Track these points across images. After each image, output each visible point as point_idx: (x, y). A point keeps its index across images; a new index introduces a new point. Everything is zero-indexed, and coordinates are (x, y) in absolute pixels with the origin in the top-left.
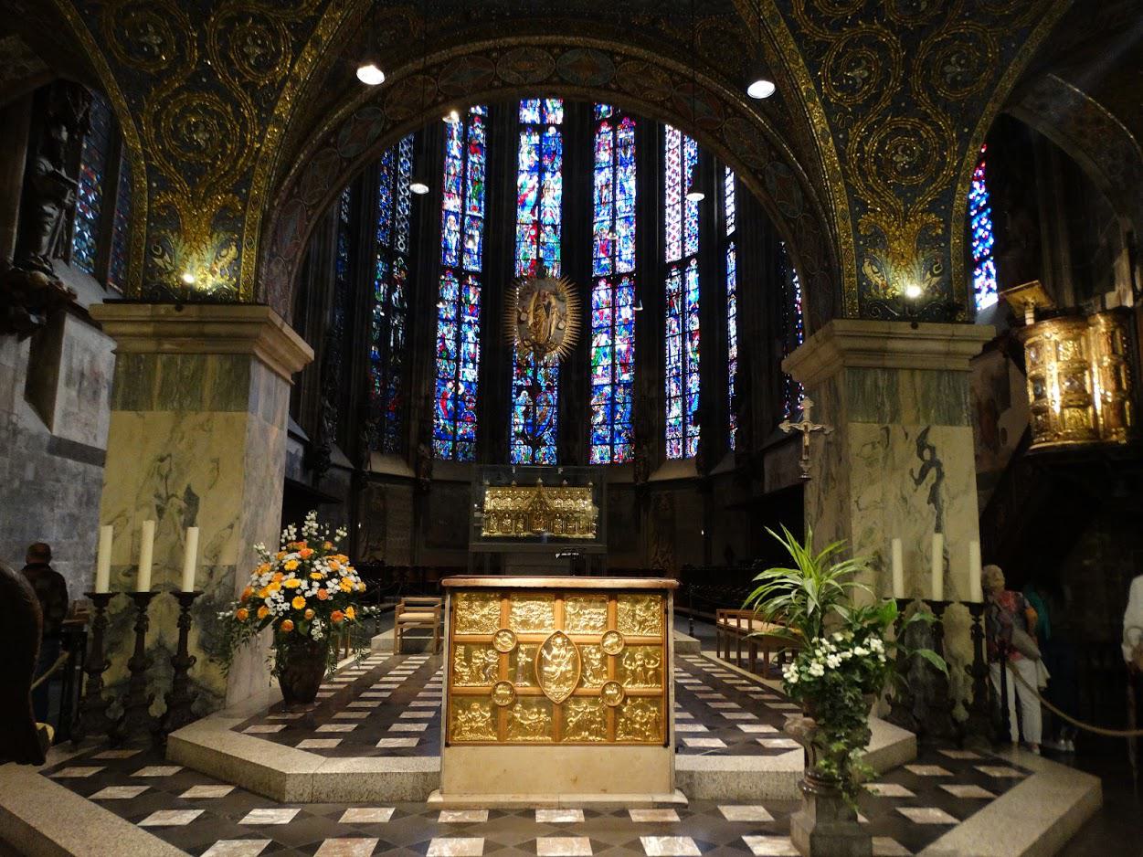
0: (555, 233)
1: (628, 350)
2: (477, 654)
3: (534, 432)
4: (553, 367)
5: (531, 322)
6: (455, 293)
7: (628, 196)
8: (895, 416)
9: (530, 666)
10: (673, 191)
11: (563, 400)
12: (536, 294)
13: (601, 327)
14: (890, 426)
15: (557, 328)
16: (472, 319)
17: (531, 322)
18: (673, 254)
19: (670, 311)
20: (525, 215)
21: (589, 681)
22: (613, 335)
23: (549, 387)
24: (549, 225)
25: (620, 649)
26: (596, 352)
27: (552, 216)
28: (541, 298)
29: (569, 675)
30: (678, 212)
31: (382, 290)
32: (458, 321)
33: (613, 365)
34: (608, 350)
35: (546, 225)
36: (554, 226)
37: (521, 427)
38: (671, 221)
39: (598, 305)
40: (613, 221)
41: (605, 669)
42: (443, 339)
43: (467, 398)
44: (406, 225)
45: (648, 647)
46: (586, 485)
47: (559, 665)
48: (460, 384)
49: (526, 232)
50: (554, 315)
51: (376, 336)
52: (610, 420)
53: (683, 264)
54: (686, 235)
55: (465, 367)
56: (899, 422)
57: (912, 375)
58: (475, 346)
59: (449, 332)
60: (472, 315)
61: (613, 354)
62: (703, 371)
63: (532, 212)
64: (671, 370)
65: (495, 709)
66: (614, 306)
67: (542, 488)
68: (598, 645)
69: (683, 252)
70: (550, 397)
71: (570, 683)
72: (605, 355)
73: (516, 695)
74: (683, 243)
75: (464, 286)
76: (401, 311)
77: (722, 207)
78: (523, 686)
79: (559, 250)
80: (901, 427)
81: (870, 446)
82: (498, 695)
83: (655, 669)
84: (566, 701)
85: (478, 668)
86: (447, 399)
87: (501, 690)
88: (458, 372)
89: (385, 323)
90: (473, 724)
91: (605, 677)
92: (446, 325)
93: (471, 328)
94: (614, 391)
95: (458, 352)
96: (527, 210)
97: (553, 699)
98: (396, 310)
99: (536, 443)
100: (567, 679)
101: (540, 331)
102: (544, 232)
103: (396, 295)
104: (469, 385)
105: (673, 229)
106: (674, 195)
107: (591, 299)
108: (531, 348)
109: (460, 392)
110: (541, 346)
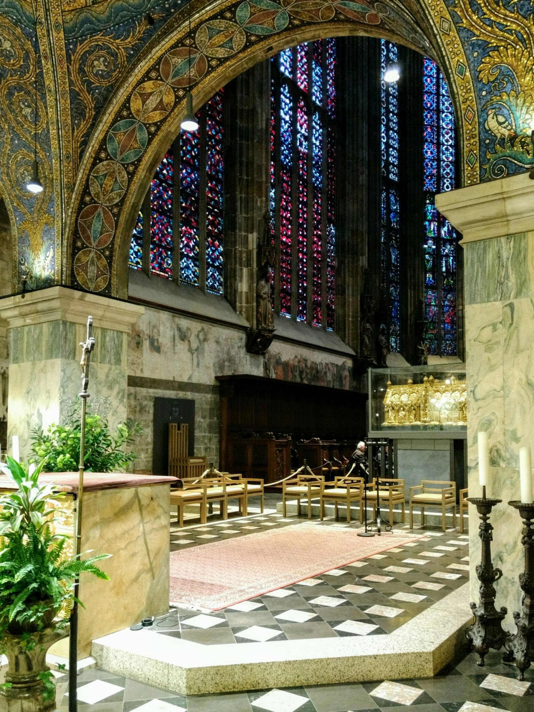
31: (432, 228)
44: (451, 170)
51: (429, 265)
80: (529, 299)
81: (491, 327)
98: (445, 241)
103: (446, 229)
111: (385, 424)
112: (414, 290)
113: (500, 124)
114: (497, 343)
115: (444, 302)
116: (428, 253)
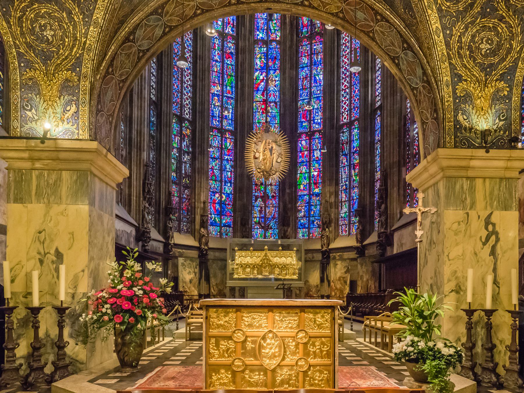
0: (276, 107)
1: (318, 175)
2: (222, 342)
3: (265, 221)
4: (275, 185)
5: (261, 158)
6: (218, 142)
7: (319, 84)
8: (473, 205)
9: (253, 349)
10: (345, 81)
11: (281, 203)
12: (264, 142)
13: (303, 162)
14: (470, 212)
15: (277, 162)
16: (229, 157)
17: (261, 158)
18: (345, 119)
19: (342, 152)
20: (259, 97)
21: (288, 357)
22: (309, 166)
23: (273, 196)
24: (272, 102)
25: (307, 340)
26: (300, 176)
27: (274, 96)
28: (267, 144)
29: (276, 354)
30: (347, 94)
32: (221, 159)
33: (310, 183)
34: (306, 175)
35: (270, 102)
36: (275, 103)
37: (258, 219)
38: (344, 99)
39: (301, 149)
40: (310, 99)
41: (298, 351)
42: (212, 169)
43: (227, 203)
45: (323, 339)
46: (293, 250)
47: (271, 349)
48: (223, 195)
49: (259, 106)
50: (275, 155)
51: (174, 167)
52: (308, 215)
53: (350, 124)
54: (352, 107)
55: (225, 185)
56: (475, 210)
57: (484, 181)
58: (231, 174)
59: (216, 165)
60: (228, 155)
61: (310, 177)
62: (362, 185)
63: (263, 95)
64: (343, 186)
65: (234, 373)
66: (311, 150)
67: (268, 252)
68: (294, 338)
69: (351, 117)
70: (274, 202)
71: (278, 358)
72: (305, 178)
73: (246, 365)
74: (351, 112)
75: (224, 139)
76: (188, 153)
77: (374, 91)
78: (250, 361)
79: (278, 117)
82: (235, 366)
83: (327, 351)
84: (275, 368)
85: (224, 351)
86: (216, 203)
87: (237, 363)
88: (221, 188)
89: (180, 162)
90: (221, 381)
91: (298, 355)
92: (214, 161)
93: (228, 163)
94: (310, 199)
95: (221, 177)
96: (260, 93)
97: (267, 367)
98: (185, 152)
99: (266, 228)
100: (275, 356)
101: (267, 163)
102: (270, 106)
104: (228, 195)
105: (345, 104)
106: (346, 83)
107: (298, 145)
108: (262, 173)
109: (223, 199)
110: (266, 172)
111: (236, 276)
112: (166, 184)
113: (465, 119)
114: (460, 231)
115: (183, 195)
116: (174, 158)
